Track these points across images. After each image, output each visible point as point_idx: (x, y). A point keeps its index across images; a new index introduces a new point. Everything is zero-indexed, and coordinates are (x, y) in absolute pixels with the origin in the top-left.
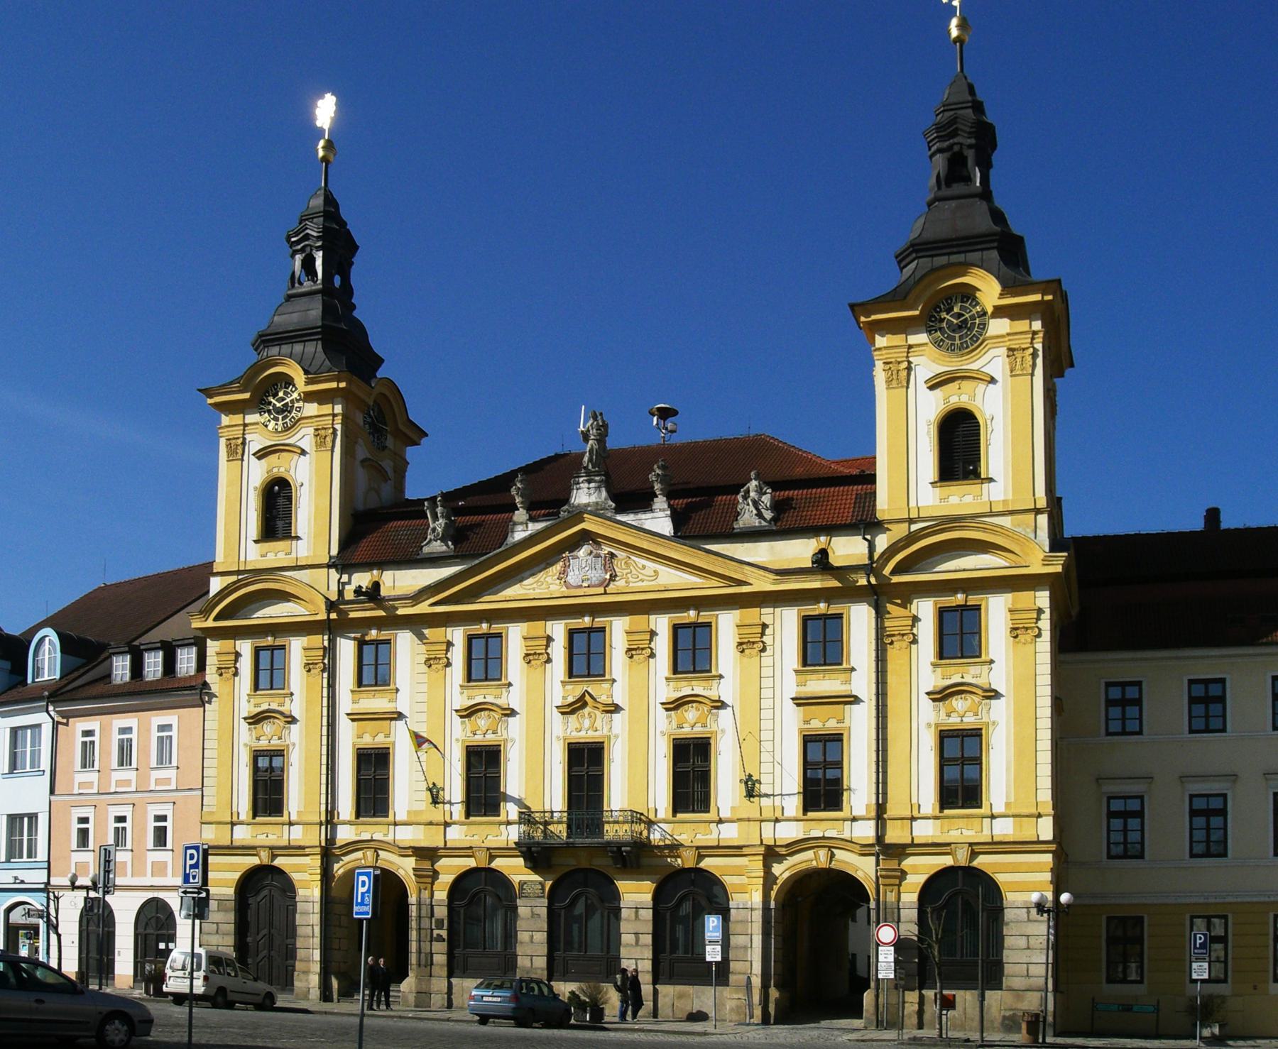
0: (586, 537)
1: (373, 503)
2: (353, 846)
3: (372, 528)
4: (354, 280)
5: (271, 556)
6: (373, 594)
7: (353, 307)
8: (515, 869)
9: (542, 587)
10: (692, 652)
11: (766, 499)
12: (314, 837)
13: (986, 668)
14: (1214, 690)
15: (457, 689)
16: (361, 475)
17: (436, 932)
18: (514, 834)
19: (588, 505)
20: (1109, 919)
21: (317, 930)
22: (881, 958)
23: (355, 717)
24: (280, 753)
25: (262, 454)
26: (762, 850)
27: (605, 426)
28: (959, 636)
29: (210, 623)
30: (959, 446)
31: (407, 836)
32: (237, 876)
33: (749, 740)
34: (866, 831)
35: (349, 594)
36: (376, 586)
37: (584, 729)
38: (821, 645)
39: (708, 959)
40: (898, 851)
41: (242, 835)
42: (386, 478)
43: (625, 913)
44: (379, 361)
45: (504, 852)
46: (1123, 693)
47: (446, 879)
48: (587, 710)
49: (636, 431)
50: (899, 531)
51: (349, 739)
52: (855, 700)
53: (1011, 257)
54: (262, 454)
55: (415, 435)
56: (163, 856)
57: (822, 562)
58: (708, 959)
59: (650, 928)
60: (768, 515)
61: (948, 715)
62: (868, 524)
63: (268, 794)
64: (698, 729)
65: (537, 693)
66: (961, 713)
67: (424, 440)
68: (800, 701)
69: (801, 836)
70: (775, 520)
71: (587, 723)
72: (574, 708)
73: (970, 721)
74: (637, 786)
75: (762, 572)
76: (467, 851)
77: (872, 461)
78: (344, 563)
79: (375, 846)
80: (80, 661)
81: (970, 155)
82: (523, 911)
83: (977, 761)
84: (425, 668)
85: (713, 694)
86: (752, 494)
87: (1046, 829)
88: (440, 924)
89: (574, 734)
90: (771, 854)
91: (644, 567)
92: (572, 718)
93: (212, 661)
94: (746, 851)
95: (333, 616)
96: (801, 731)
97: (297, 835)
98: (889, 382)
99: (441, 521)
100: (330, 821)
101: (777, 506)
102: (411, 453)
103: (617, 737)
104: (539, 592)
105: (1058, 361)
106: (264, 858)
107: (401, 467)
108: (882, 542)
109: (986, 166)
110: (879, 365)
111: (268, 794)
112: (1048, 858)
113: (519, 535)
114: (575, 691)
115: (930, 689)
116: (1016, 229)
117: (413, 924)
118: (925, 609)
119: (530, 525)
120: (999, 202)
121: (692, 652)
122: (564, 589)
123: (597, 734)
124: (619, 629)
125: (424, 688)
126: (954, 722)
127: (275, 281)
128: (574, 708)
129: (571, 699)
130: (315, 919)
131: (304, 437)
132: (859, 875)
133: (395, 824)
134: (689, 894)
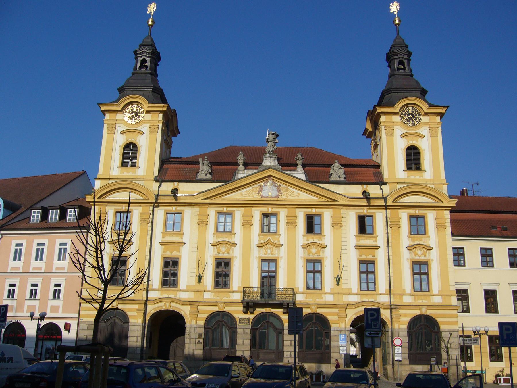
3: (172, 167)
13: (427, 239)
14: (489, 252)
22: (396, 352)
28: (418, 225)
38: (363, 225)
39: (341, 352)
46: (486, 252)
52: (377, 247)
58: (341, 352)
61: (415, 256)
66: (420, 255)
69: (360, 301)
71: (269, 251)
73: (423, 258)
84: (196, 225)
89: (264, 255)
90: (347, 306)
96: (358, 259)
103: (281, 257)
104: (240, 197)
119: (246, 171)
122: (260, 197)
123: (274, 256)
125: (197, 233)
126: (417, 258)
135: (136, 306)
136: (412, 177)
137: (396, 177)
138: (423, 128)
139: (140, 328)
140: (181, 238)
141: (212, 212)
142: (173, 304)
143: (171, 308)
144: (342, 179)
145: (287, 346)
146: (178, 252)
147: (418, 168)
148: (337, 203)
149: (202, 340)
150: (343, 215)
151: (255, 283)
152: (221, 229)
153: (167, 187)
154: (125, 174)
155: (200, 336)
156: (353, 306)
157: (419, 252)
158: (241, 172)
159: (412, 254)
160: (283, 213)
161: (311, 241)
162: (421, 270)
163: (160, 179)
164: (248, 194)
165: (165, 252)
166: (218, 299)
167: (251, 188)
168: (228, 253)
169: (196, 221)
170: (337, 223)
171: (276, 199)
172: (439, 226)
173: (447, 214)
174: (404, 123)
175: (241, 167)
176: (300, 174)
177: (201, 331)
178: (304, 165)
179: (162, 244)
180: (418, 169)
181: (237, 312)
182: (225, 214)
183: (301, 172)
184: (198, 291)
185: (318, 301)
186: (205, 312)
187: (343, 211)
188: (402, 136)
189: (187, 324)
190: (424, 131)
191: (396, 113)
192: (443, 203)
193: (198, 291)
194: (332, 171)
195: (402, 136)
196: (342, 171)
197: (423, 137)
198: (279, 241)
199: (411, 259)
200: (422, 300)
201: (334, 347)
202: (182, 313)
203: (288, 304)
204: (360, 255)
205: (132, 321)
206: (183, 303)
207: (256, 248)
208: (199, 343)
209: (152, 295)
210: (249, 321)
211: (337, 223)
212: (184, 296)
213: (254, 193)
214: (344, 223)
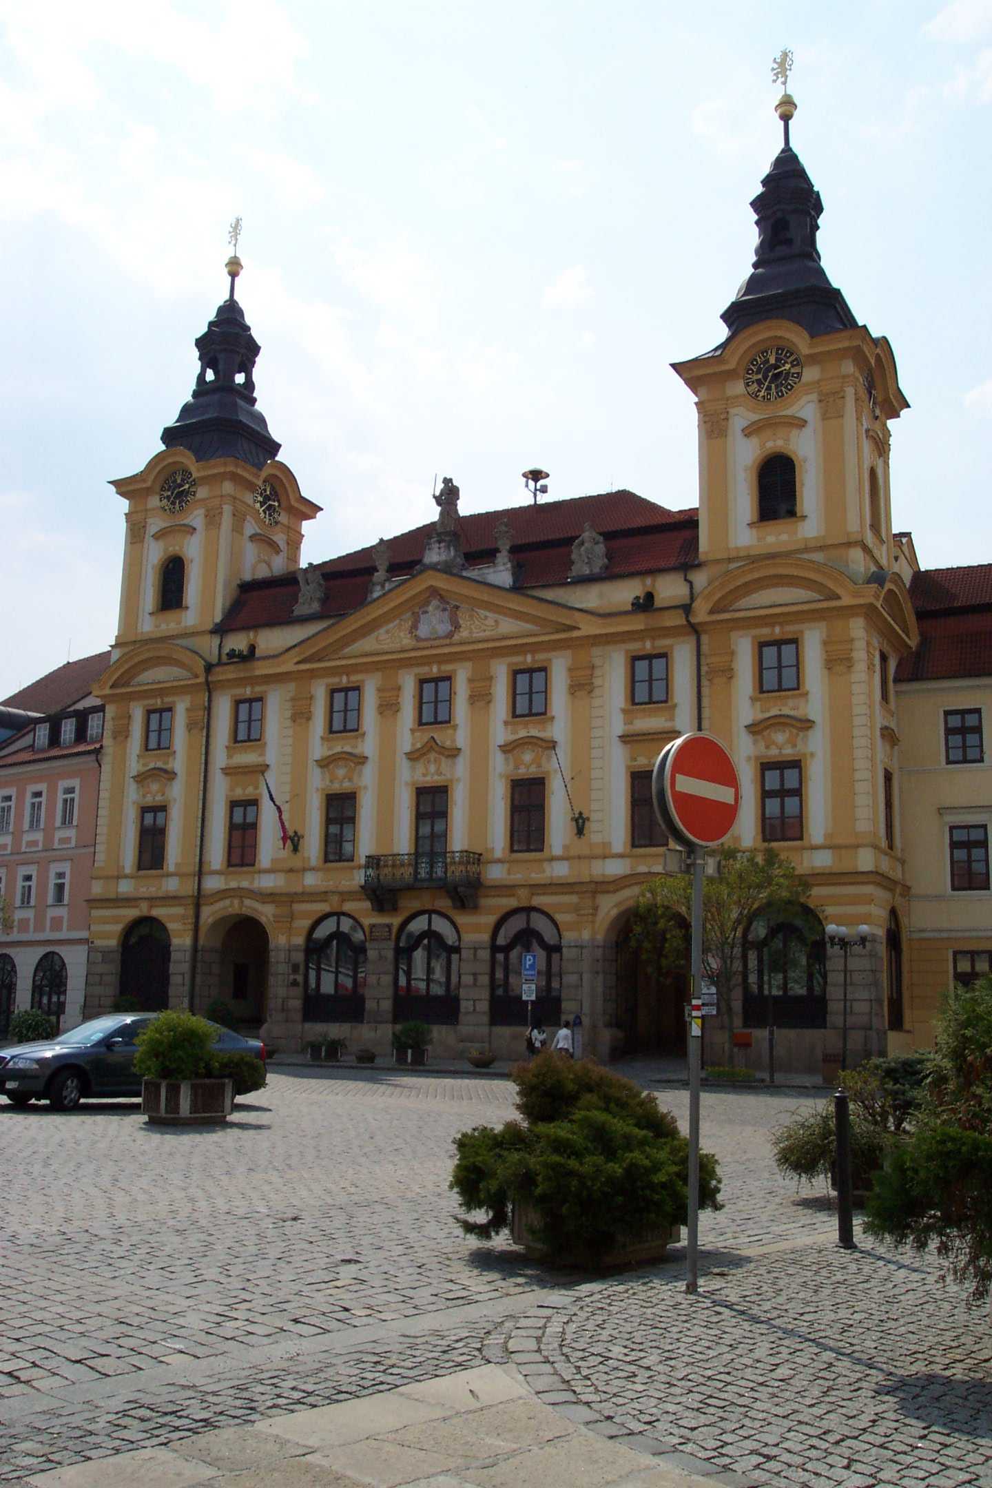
0: (434, 592)
1: (262, 573)
4: (255, 378)
5: (163, 626)
6: (250, 656)
18: (359, 878)
19: (438, 563)
23: (227, 771)
24: (163, 808)
29: (107, 691)
32: (118, 928)
33: (581, 777)
36: (252, 648)
45: (345, 896)
48: (432, 756)
51: (221, 791)
55: (311, 510)
56: (62, 912)
57: (646, 604)
61: (767, 747)
62: (688, 562)
64: (533, 769)
65: (388, 740)
66: (781, 745)
67: (319, 514)
71: (432, 768)
73: (788, 752)
75: (589, 617)
76: (322, 896)
78: (221, 630)
83: (798, 792)
89: (421, 779)
90: (601, 887)
91: (486, 617)
93: (109, 725)
96: (628, 767)
100: (201, 872)
102: (307, 526)
103: (458, 780)
106: (141, 910)
107: (295, 541)
108: (700, 579)
113: (376, 595)
114: (423, 737)
115: (749, 722)
122: (414, 643)
124: (462, 676)
129: (419, 745)
130: (186, 967)
133: (260, 872)
134: (524, 933)
135: (179, 910)
136: (771, 539)
137: (732, 545)
138: (805, 399)
139: (188, 956)
140: (262, 754)
142: (247, 902)
143: (244, 911)
144: (596, 570)
145: (466, 986)
146: (256, 788)
148: (575, 634)
149: (300, 978)
150: (597, 662)
151: (403, 843)
152: (337, 725)
153: (238, 642)
154: (163, 626)
155: (295, 968)
156: (611, 888)
157: (780, 737)
158: (378, 588)
159: (762, 745)
161: (522, 733)
164: (391, 638)
165: (232, 789)
166: (330, 885)
168: (350, 780)
169: (288, 714)
170: (582, 686)
171: (448, 641)
172: (837, 661)
173: (858, 628)
176: (501, 574)
177: (299, 957)
178: (515, 550)
179: (227, 771)
183: (502, 568)
184: (291, 870)
185: (536, 877)
187: (596, 651)
188: (748, 432)
190: (805, 407)
191: (730, 375)
192: (839, 598)
193: (291, 870)
194: (574, 556)
195: (748, 432)
196: (600, 549)
197: (802, 424)
198: (454, 741)
199: (757, 758)
202: (263, 920)
203: (455, 888)
205: (175, 941)
206: (269, 897)
208: (295, 983)
209: (213, 884)
210: (390, 931)
211: (582, 686)
212: (267, 882)
213: (402, 634)
214: (597, 682)
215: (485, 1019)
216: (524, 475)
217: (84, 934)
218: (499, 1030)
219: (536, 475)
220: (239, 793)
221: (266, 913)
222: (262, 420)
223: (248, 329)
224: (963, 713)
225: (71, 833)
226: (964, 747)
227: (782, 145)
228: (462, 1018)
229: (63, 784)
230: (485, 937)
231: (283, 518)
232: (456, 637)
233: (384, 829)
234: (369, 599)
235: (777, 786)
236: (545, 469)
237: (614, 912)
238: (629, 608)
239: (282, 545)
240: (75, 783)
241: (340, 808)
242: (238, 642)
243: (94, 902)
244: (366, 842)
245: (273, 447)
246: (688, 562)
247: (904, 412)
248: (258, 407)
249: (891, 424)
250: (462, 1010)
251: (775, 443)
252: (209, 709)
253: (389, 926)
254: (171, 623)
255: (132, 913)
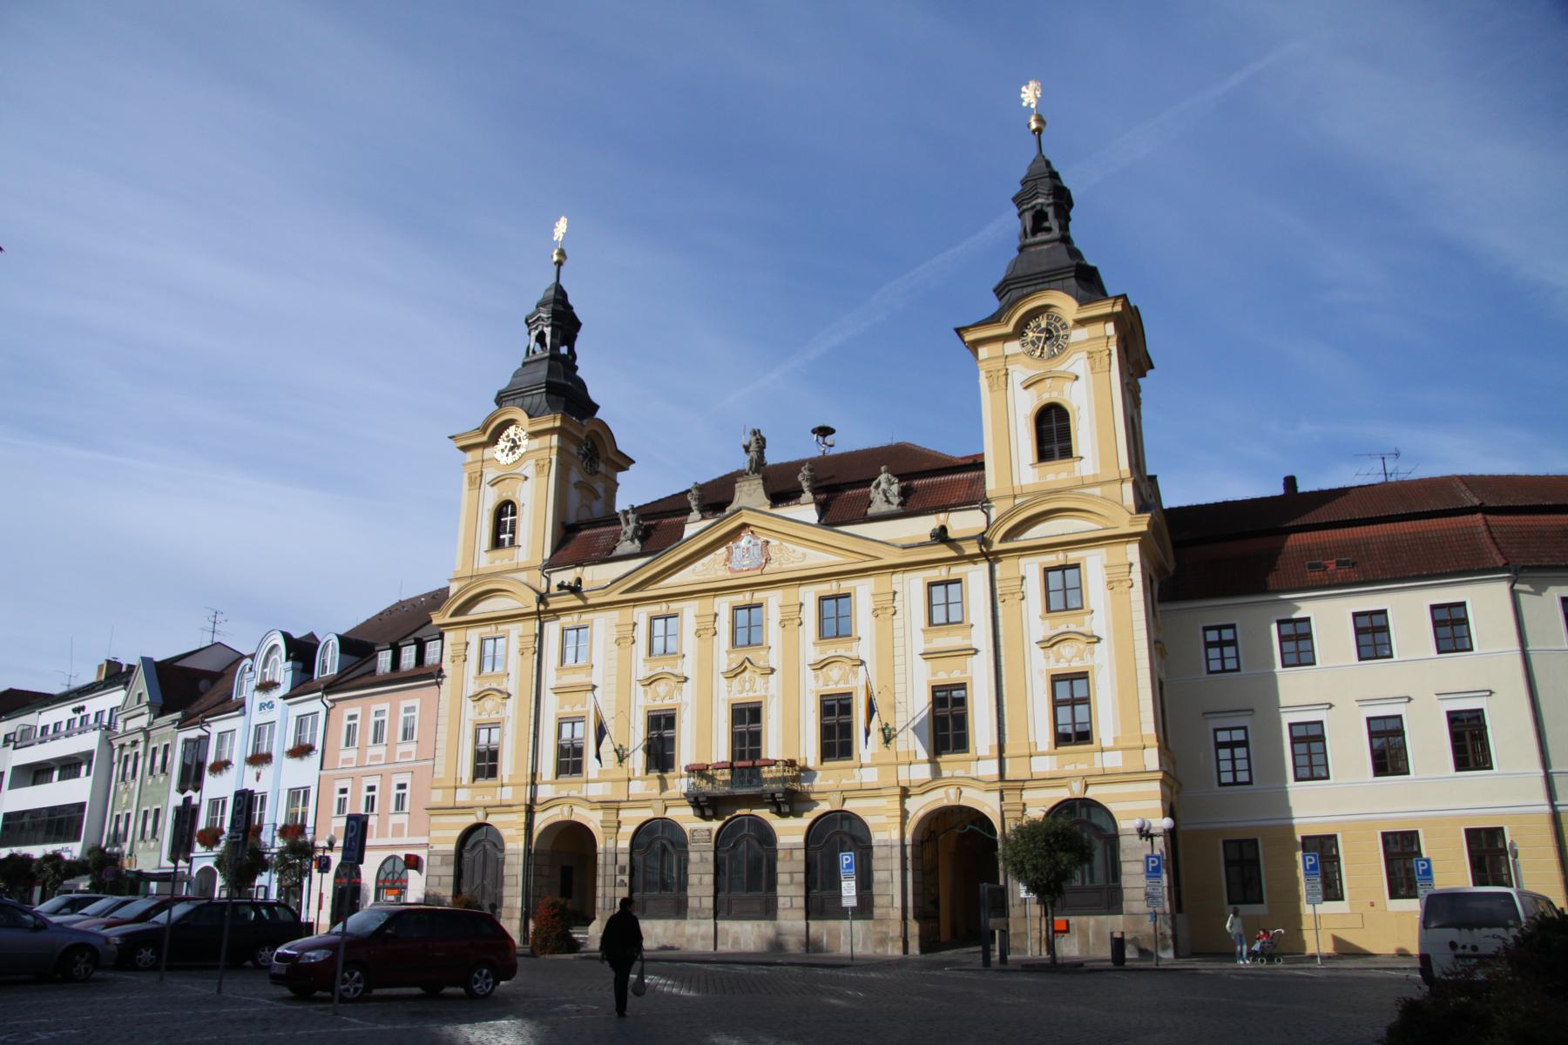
2: (551, 803)
3: (581, 533)
6: (575, 589)
7: (576, 368)
8: (685, 817)
9: (709, 570)
10: (834, 620)
11: (895, 488)
12: (524, 796)
15: (641, 662)
16: (574, 496)
17: (619, 878)
20: (1225, 843)
21: (520, 879)
23: (559, 691)
25: (494, 484)
26: (898, 791)
27: (764, 440)
28: (1063, 589)
29: (448, 620)
30: (1052, 431)
31: (597, 791)
32: (457, 833)
34: (990, 769)
35: (554, 590)
36: (579, 581)
37: (746, 690)
40: (1020, 785)
41: (463, 796)
42: (597, 497)
43: (780, 854)
44: (596, 407)
47: (628, 830)
48: (746, 675)
49: (790, 446)
50: (1007, 505)
51: (552, 707)
53: (1087, 282)
54: (494, 484)
55: (625, 462)
57: (941, 536)
59: (802, 867)
60: (896, 500)
62: (975, 498)
63: (486, 764)
65: (706, 663)
66: (1068, 659)
67: (632, 467)
68: (928, 655)
70: (901, 504)
71: (747, 686)
72: (735, 674)
74: (791, 737)
77: (982, 455)
78: (553, 564)
79: (571, 801)
80: (355, 659)
81: (1050, 211)
82: (693, 856)
85: (853, 654)
86: (883, 486)
87: (1152, 759)
88: (622, 870)
92: (736, 681)
94: (883, 792)
95: (542, 607)
97: (507, 795)
98: (991, 386)
99: (632, 525)
101: (905, 493)
105: (1135, 361)
106: (478, 817)
109: (1064, 219)
110: (982, 374)
111: (486, 764)
112: (1156, 786)
114: (738, 657)
116: (1090, 261)
117: (600, 871)
118: (1031, 567)
120: (1077, 244)
121: (834, 620)
126: (1063, 667)
127: (510, 350)
128: (735, 674)
131: (529, 469)
132: (986, 811)
134: (839, 835)
138: (1075, 357)
140: (590, 675)
141: (641, 614)
144: (894, 508)
147: (1067, 453)
151: (721, 751)
153: (568, 576)
155: (622, 870)
160: (773, 600)
162: (1070, 691)
163: (553, 564)
167: (711, 556)
174: (1030, 354)
175: (695, 515)
176: (806, 511)
177: (624, 859)
178: (815, 491)
179: (559, 691)
180: (1067, 453)
181: (685, 817)
182: (946, 583)
185: (846, 783)
186: (632, 820)
187: (897, 578)
189: (600, 847)
190: (1076, 362)
200: (1076, 760)
201: (880, 883)
202: (591, 826)
204: (934, 674)
205: (509, 846)
207: (810, 673)
209: (544, 792)
211: (886, 609)
215: (802, 913)
216: (814, 432)
217: (424, 840)
218: (815, 926)
219: (824, 431)
220: (568, 711)
221: (593, 820)
222: (581, 385)
223: (571, 308)
224: (1219, 628)
225: (411, 747)
226: (1222, 658)
227: (1034, 153)
228: (780, 914)
229: (404, 704)
230: (800, 839)
231: (602, 468)
232: (767, 569)
233: (704, 742)
234: (685, 536)
235: (1068, 696)
236: (831, 425)
237: (922, 813)
238: (928, 539)
239: (601, 491)
240: (416, 702)
241: (662, 725)
242: (568, 576)
243: (436, 810)
244: (686, 753)
245: (595, 408)
246: (975, 498)
247: (1149, 373)
248: (579, 373)
249: (1141, 381)
250: (780, 905)
251: (1048, 394)
252: (540, 636)
253: (710, 831)
254: (503, 559)
255: (471, 820)
